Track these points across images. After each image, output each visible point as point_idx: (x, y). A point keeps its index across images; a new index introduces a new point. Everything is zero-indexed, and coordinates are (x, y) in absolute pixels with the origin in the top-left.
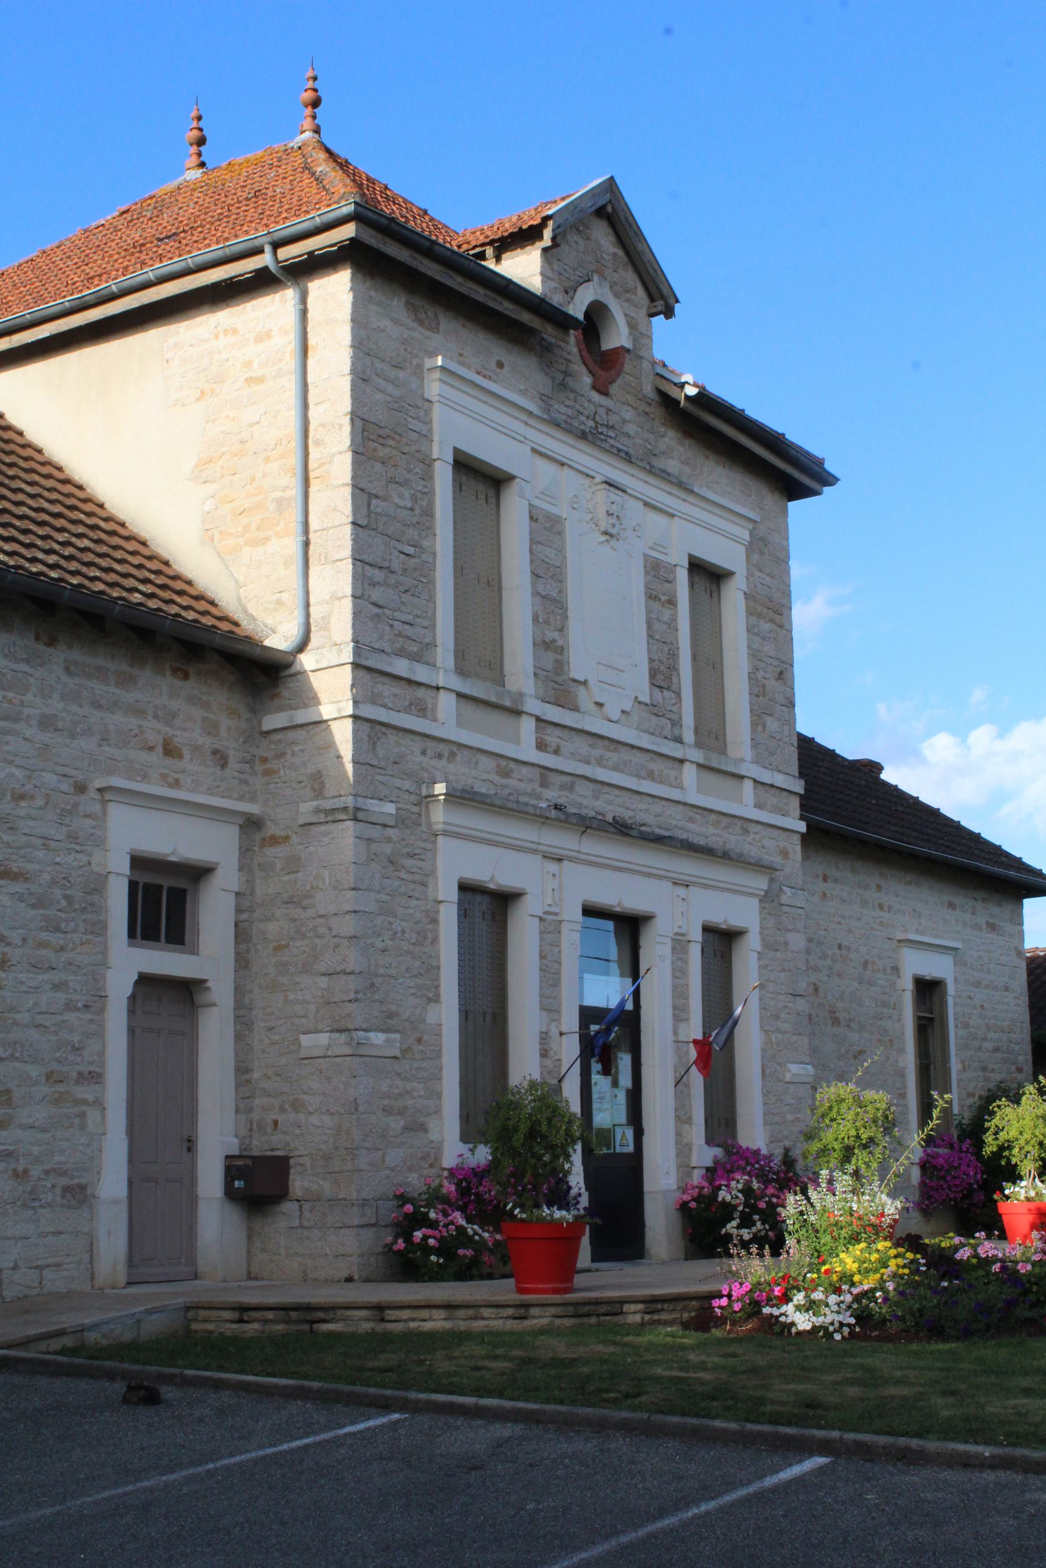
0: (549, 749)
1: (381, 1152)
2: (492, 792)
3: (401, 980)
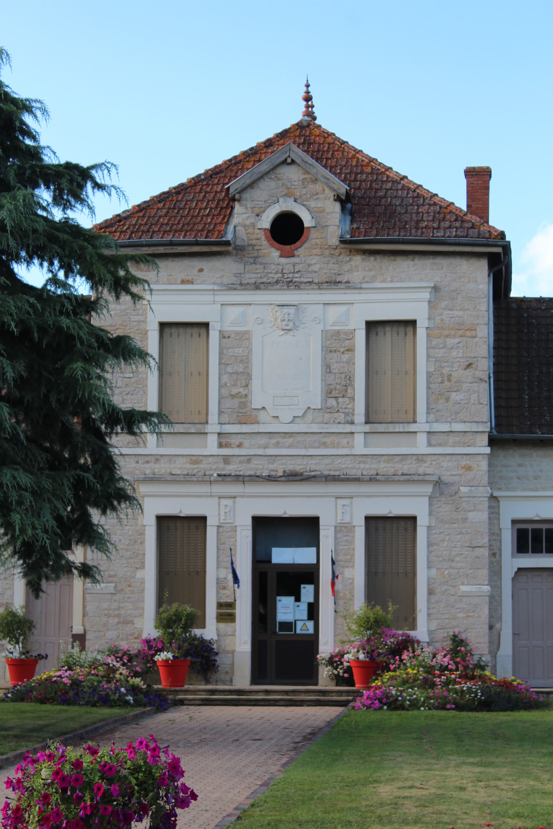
0: (232, 446)
1: (103, 633)
2: (185, 473)
3: (117, 561)
